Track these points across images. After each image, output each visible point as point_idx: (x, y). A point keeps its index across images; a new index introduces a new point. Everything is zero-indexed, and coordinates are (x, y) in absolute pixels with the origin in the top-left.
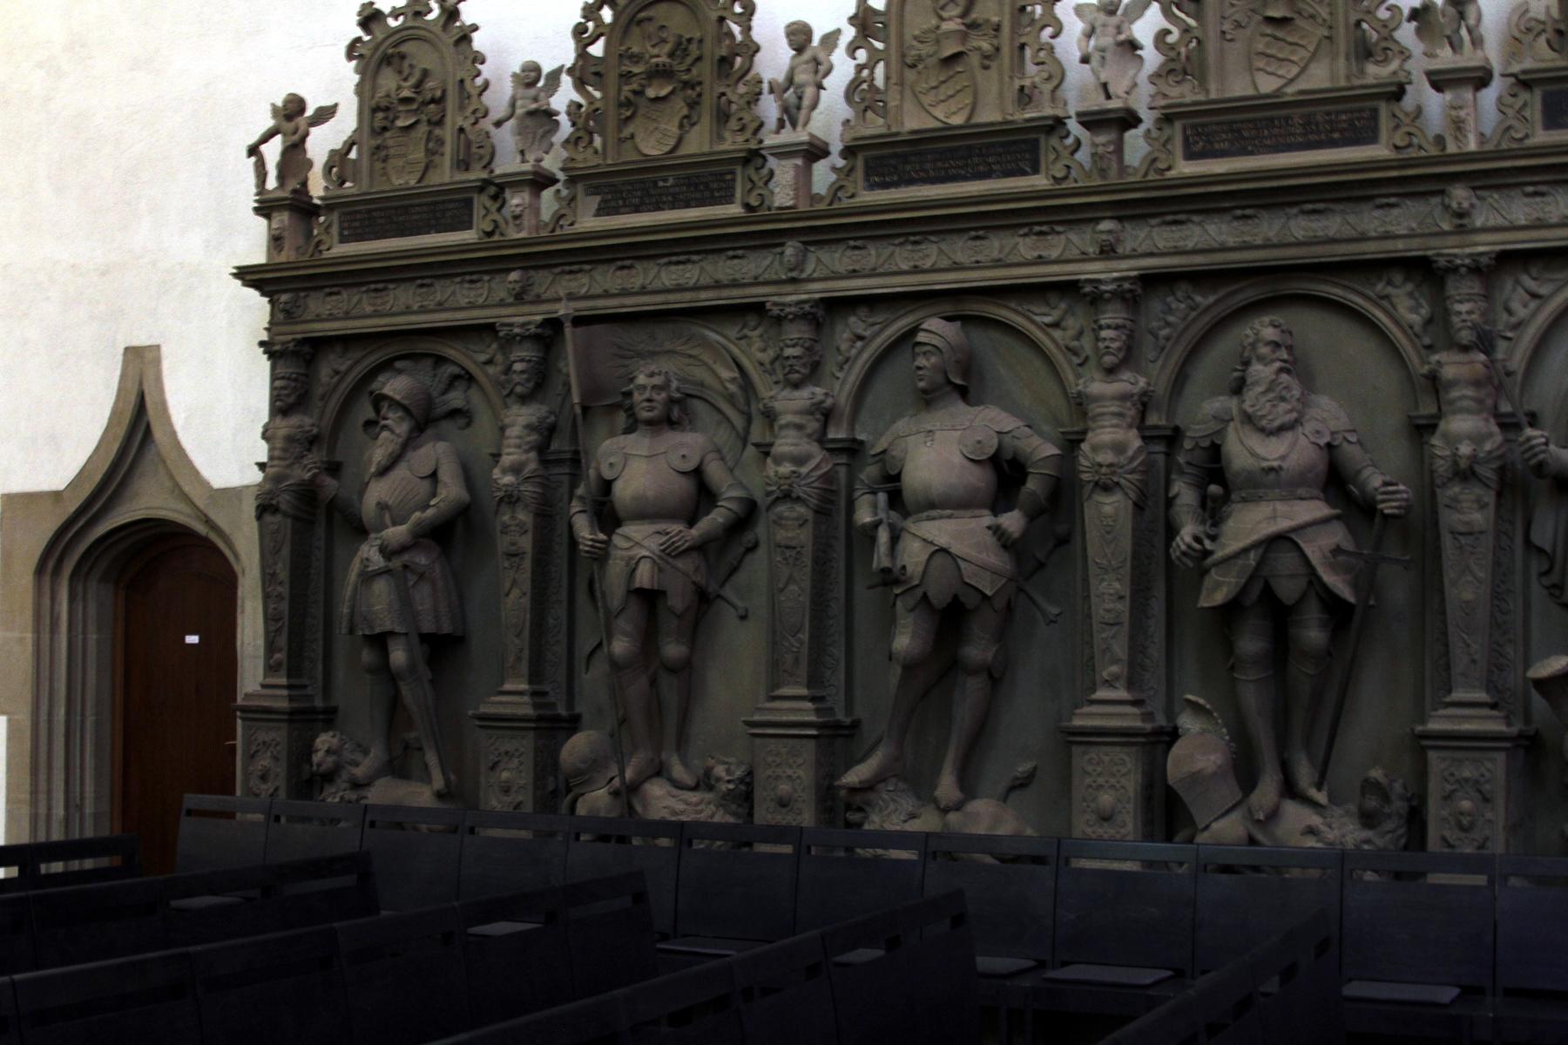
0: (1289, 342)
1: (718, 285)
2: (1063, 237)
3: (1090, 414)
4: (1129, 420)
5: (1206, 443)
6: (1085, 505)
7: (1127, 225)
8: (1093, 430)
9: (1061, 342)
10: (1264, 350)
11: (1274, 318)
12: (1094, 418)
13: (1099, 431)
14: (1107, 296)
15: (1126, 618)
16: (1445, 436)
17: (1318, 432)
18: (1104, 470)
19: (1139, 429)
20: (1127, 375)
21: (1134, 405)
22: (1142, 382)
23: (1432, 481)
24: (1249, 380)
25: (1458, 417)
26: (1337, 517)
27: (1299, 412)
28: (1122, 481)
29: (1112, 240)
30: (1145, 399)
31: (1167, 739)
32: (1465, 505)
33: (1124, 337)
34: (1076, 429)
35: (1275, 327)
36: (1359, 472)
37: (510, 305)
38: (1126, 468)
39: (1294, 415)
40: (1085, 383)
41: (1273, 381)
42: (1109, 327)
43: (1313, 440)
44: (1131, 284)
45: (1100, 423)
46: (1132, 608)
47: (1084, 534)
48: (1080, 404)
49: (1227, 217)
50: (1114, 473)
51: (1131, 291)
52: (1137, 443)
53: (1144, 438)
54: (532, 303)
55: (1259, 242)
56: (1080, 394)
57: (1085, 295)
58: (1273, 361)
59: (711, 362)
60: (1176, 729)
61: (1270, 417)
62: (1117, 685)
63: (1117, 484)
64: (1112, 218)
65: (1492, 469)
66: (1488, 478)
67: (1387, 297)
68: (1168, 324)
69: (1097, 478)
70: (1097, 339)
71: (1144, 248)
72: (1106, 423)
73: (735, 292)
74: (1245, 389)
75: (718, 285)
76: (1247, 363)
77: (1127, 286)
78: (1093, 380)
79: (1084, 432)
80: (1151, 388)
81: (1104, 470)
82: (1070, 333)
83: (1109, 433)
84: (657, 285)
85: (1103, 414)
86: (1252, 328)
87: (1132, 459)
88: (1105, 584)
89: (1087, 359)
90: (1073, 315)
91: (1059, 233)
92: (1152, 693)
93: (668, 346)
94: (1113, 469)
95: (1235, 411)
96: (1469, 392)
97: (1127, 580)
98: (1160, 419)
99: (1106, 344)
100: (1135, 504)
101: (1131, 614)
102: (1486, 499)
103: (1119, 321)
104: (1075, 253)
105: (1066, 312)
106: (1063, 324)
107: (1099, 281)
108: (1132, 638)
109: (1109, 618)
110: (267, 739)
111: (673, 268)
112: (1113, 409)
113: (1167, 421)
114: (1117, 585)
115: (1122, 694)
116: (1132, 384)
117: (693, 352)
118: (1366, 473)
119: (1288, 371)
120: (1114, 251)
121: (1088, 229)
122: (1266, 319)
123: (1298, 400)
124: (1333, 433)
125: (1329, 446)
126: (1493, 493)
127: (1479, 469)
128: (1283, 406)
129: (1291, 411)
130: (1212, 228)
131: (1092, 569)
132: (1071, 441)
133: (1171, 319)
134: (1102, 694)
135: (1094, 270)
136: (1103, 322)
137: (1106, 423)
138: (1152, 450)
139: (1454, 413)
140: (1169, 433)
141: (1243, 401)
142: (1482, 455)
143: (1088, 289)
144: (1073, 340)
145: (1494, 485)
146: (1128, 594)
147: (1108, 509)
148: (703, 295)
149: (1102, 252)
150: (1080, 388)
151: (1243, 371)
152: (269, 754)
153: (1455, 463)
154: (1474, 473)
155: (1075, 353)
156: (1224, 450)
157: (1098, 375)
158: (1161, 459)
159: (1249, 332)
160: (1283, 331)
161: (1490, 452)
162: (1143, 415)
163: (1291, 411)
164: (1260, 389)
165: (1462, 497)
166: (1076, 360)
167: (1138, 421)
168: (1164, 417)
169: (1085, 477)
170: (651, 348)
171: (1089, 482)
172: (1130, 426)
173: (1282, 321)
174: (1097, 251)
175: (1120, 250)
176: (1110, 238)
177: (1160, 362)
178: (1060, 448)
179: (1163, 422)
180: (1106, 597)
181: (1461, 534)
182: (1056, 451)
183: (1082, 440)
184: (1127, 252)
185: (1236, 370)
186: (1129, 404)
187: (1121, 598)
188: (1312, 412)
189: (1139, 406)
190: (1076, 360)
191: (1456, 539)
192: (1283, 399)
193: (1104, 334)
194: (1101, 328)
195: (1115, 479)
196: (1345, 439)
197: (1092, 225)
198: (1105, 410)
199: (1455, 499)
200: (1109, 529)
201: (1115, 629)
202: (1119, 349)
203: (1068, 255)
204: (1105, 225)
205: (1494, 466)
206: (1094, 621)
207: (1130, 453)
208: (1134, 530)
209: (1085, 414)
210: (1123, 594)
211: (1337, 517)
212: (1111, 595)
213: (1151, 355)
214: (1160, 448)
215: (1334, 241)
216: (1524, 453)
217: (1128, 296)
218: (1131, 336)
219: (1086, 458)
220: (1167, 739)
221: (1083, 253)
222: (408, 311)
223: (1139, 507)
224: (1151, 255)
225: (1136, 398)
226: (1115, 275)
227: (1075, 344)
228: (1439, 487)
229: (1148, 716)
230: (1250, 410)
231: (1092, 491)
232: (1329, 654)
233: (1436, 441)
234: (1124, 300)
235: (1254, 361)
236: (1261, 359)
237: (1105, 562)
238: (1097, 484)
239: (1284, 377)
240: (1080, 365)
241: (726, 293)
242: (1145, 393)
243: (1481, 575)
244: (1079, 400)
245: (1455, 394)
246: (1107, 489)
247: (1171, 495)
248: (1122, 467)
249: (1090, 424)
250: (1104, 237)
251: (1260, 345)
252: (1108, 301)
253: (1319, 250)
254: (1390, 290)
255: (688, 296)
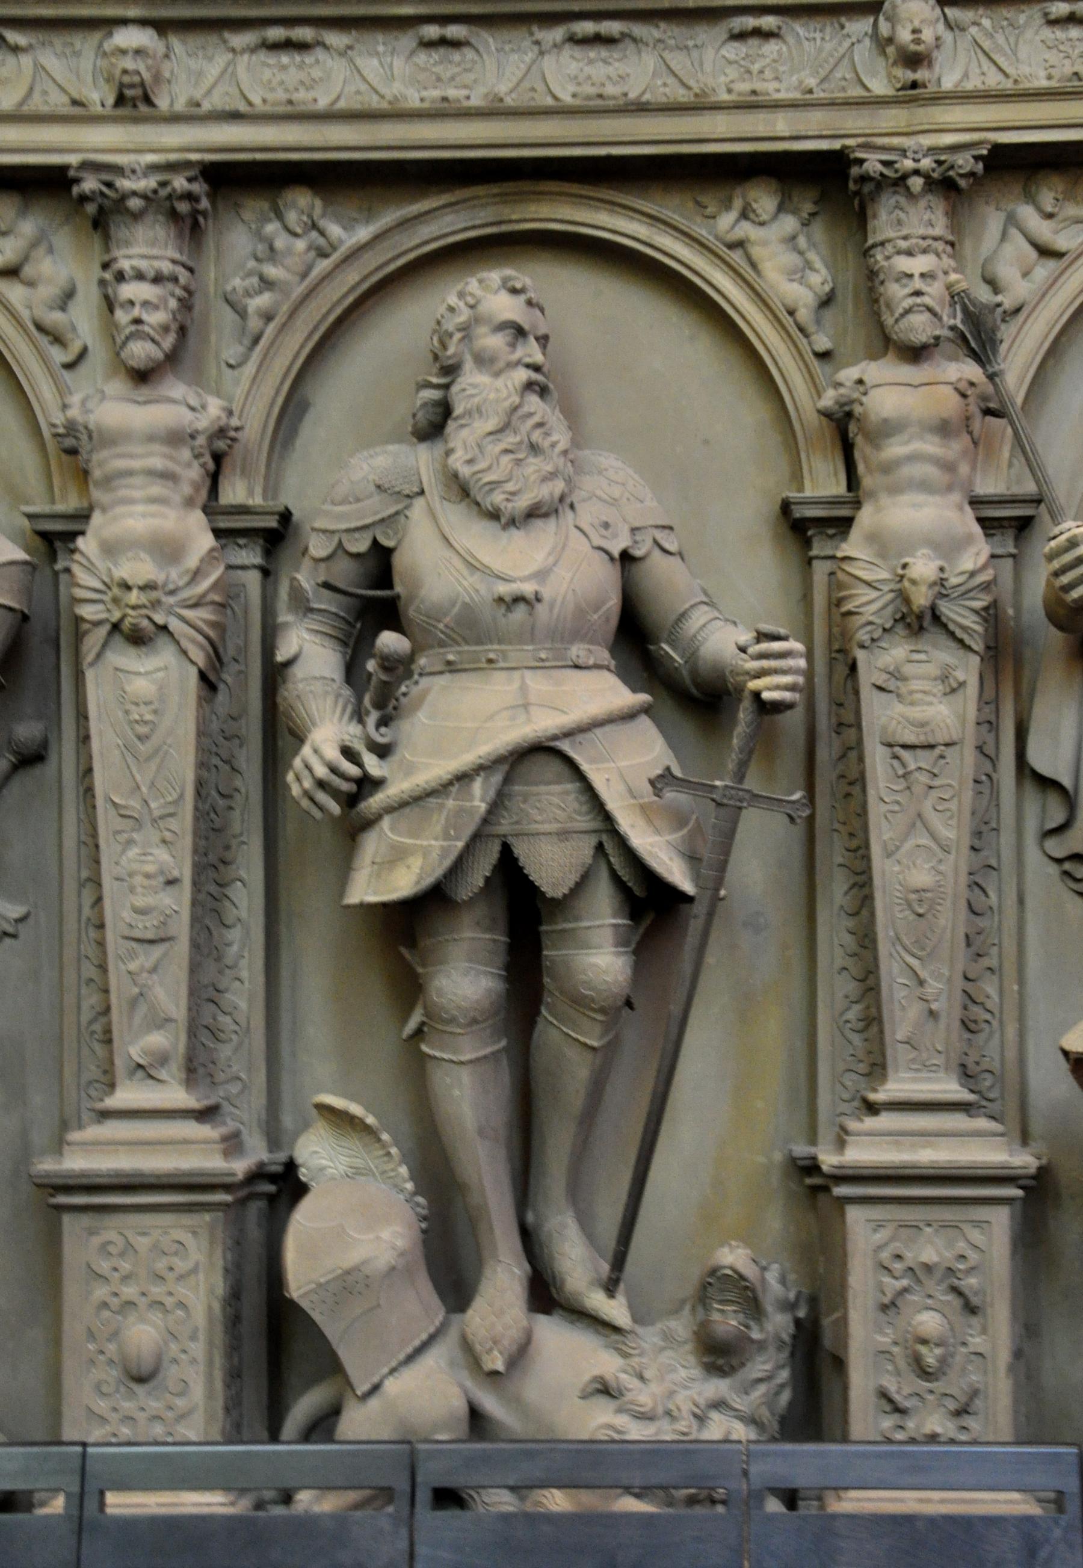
0: (541, 331)
2: (26, 60)
3: (97, 473)
4: (187, 489)
5: (361, 545)
6: (90, 675)
7: (175, 41)
8: (104, 510)
9: (25, 314)
10: (494, 342)
11: (509, 272)
12: (108, 481)
13: (120, 510)
14: (135, 203)
15: (182, 928)
16: (873, 538)
17: (606, 525)
18: (134, 597)
19: (205, 510)
20: (176, 388)
21: (197, 456)
22: (214, 407)
23: (846, 635)
24: (458, 410)
25: (906, 498)
26: (646, 710)
27: (569, 481)
28: (174, 624)
29: (147, 76)
30: (221, 445)
31: (271, 1188)
32: (915, 685)
33: (173, 303)
34: (60, 508)
35: (514, 291)
36: (683, 615)
38: (185, 594)
39: (558, 486)
40: (83, 402)
41: (515, 409)
42: (140, 276)
43: (598, 541)
44: (190, 180)
45: (123, 493)
46: (194, 903)
47: (84, 739)
48: (73, 452)
49: (407, 40)
50: (156, 604)
51: (189, 197)
52: (207, 541)
53: (218, 533)
55: (476, 101)
56: (71, 427)
57: (83, 199)
58: (512, 365)
60: (291, 1166)
61: (510, 487)
62: (163, 1074)
63: (164, 628)
64: (143, 22)
65: (976, 612)
66: (964, 628)
67: (739, 245)
68: (267, 284)
69: (116, 616)
70: (110, 304)
71: (216, 101)
72: (137, 494)
74: (451, 425)
76: (451, 370)
77: (180, 183)
78: (103, 396)
79: (83, 516)
80: (235, 422)
81: (134, 597)
82: (47, 292)
83: (144, 515)
85: (130, 473)
86: (461, 295)
87: (196, 575)
88: (133, 852)
89: (83, 353)
90: (51, 250)
91: (16, 49)
92: (234, 1089)
94: (154, 595)
95: (428, 477)
96: (931, 446)
97: (188, 841)
98: (251, 493)
99: (136, 312)
100: (203, 676)
101: (195, 920)
102: (960, 675)
103: (166, 267)
104: (58, 102)
105: (34, 245)
106: (28, 271)
107: (117, 170)
108: (194, 968)
109: (146, 927)
112: (157, 463)
113: (265, 497)
114: (162, 855)
115: (177, 1096)
116: (192, 409)
118: (698, 618)
119: (543, 391)
120: (148, 100)
121: (86, 44)
122: (495, 276)
123: (565, 453)
124: (634, 530)
125: (626, 558)
126: (975, 661)
127: (946, 609)
128: (535, 466)
129: (552, 476)
130: (370, 66)
131: (105, 819)
132: (47, 537)
133: (272, 271)
134: (127, 1096)
136: (125, 265)
137: (137, 494)
138: (239, 561)
139: (895, 490)
140: (272, 523)
141: (448, 453)
142: (954, 581)
143: (90, 184)
144: (51, 308)
145: (978, 645)
146: (186, 874)
147: (141, 687)
149: (121, 100)
150: (74, 413)
151: (447, 387)
153: (903, 597)
154: (936, 618)
155: (58, 339)
156: (399, 561)
157: (118, 386)
158: (253, 579)
159: (453, 300)
160: (530, 303)
161: (972, 574)
162: (214, 479)
163: (552, 476)
164: (491, 424)
165: (908, 669)
166: (58, 356)
167: (204, 493)
168: (258, 490)
169: (87, 612)
171: (97, 624)
172: (189, 503)
173: (528, 281)
174: (111, 100)
175: (163, 103)
176: (141, 67)
177: (250, 368)
178: (27, 550)
179: (257, 501)
180: (138, 880)
181: (905, 747)
182: (21, 555)
183: (82, 533)
184: (180, 106)
185: (429, 385)
186: (186, 454)
187: (171, 882)
188: (589, 484)
189: (208, 459)
190: (58, 356)
191: (896, 757)
192: (534, 449)
193: (128, 290)
194: (120, 277)
195: (160, 619)
196: (656, 543)
197: (97, 36)
198: (136, 464)
199: (896, 674)
200: (143, 730)
201: (157, 951)
202: (166, 329)
203: (37, 104)
204: (129, 38)
205: (978, 604)
206: (111, 936)
207: (192, 561)
208: (200, 734)
209: (84, 475)
210: (176, 873)
211: (646, 710)
212: (148, 876)
213: (232, 352)
214: (251, 555)
215: (640, 108)
216: (1057, 574)
217: (183, 207)
218: (186, 304)
219: (90, 569)
220: (271, 1188)
221: (75, 102)
223: (208, 683)
224: (235, 116)
225: (201, 440)
226: (151, 158)
227: (55, 318)
228: (862, 646)
229: (232, 1144)
230: (465, 471)
231: (105, 645)
232: (629, 1004)
233: (853, 546)
234: (174, 215)
235: (468, 365)
236: (483, 361)
237: (135, 803)
238: (116, 627)
239: (533, 401)
240: (69, 366)
242: (221, 432)
243: (948, 833)
244: (69, 442)
245: (895, 449)
246: (137, 639)
247: (280, 657)
248: (172, 593)
249: (97, 494)
250: (129, 63)
251: (482, 330)
252: (136, 216)
254: (746, 230)
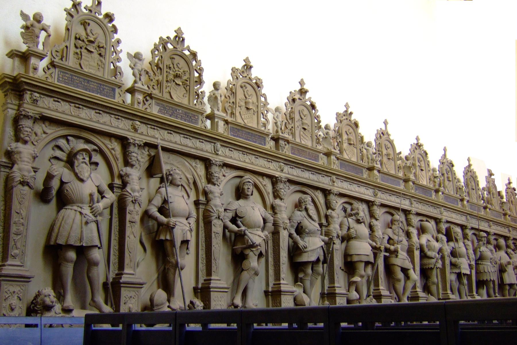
1: (196, 149)
37: (132, 132)
54: (139, 134)
59: (184, 171)
73: (201, 152)
75: (196, 149)
84: (179, 142)
93: (172, 162)
110: (15, 291)
111: (184, 139)
117: (179, 166)
135: (277, 174)
148: (193, 150)
152: (16, 298)
170: (167, 161)
222: (90, 120)
241: (199, 152)
253: (310, 181)
255: (188, 149)
